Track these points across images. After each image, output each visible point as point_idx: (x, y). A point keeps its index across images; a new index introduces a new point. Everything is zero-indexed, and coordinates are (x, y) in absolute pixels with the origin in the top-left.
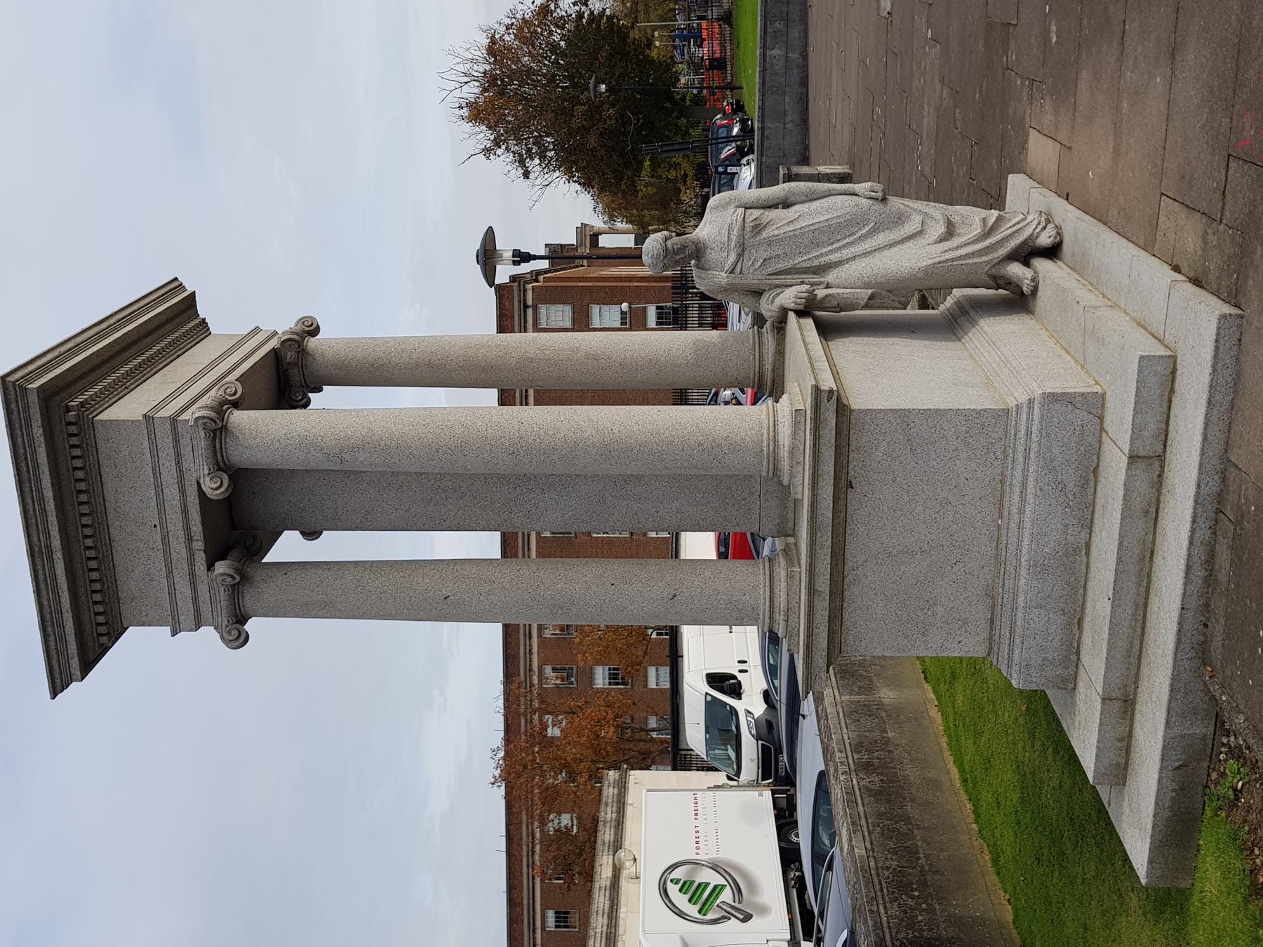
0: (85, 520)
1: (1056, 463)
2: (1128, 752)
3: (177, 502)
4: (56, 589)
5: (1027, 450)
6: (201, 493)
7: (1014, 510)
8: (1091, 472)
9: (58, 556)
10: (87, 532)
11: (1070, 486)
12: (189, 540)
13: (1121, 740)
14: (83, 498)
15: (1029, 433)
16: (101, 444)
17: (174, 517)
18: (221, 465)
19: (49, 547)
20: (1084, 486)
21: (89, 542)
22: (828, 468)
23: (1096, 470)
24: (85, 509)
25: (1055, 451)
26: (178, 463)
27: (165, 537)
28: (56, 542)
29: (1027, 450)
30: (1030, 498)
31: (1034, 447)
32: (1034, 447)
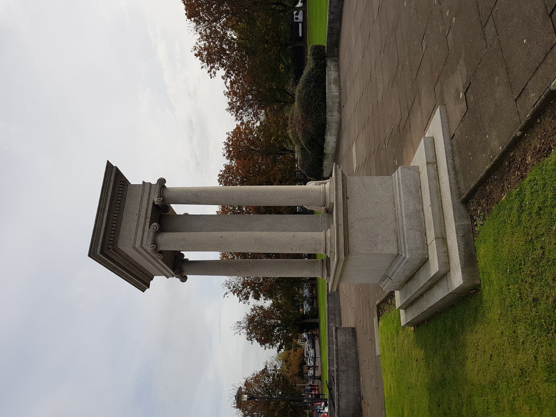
0: (117, 208)
1: (408, 185)
2: (448, 256)
3: (145, 207)
4: (102, 222)
5: (399, 184)
6: (154, 203)
7: (398, 202)
8: (419, 188)
9: (106, 213)
10: (116, 212)
11: (414, 192)
12: (146, 218)
13: (445, 253)
14: (119, 202)
15: (398, 179)
16: (128, 191)
17: (143, 211)
18: (161, 195)
19: (104, 209)
20: (418, 192)
21: (116, 215)
22: (340, 187)
23: (420, 187)
24: (118, 205)
25: (407, 182)
26: (149, 195)
27: (139, 216)
28: (107, 209)
29: (399, 184)
30: (402, 196)
31: (401, 181)
32: (401, 181)
